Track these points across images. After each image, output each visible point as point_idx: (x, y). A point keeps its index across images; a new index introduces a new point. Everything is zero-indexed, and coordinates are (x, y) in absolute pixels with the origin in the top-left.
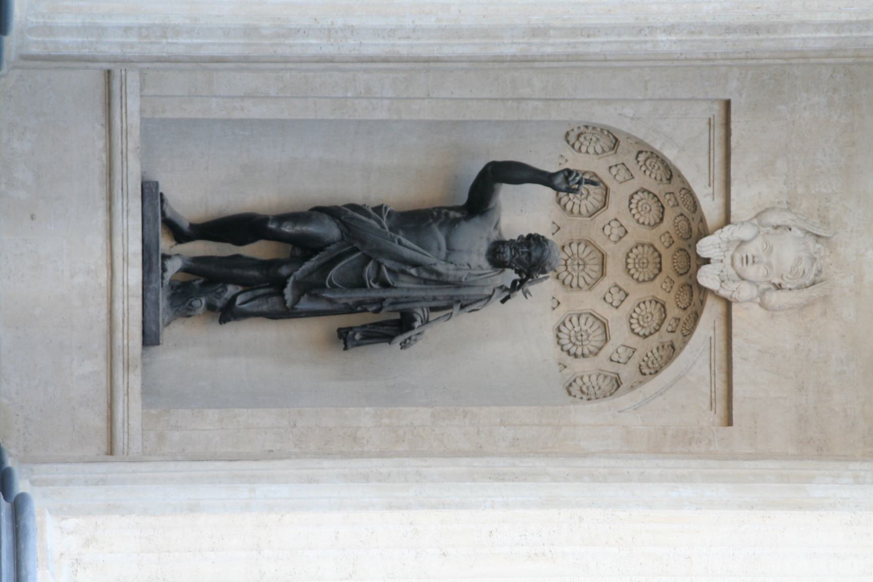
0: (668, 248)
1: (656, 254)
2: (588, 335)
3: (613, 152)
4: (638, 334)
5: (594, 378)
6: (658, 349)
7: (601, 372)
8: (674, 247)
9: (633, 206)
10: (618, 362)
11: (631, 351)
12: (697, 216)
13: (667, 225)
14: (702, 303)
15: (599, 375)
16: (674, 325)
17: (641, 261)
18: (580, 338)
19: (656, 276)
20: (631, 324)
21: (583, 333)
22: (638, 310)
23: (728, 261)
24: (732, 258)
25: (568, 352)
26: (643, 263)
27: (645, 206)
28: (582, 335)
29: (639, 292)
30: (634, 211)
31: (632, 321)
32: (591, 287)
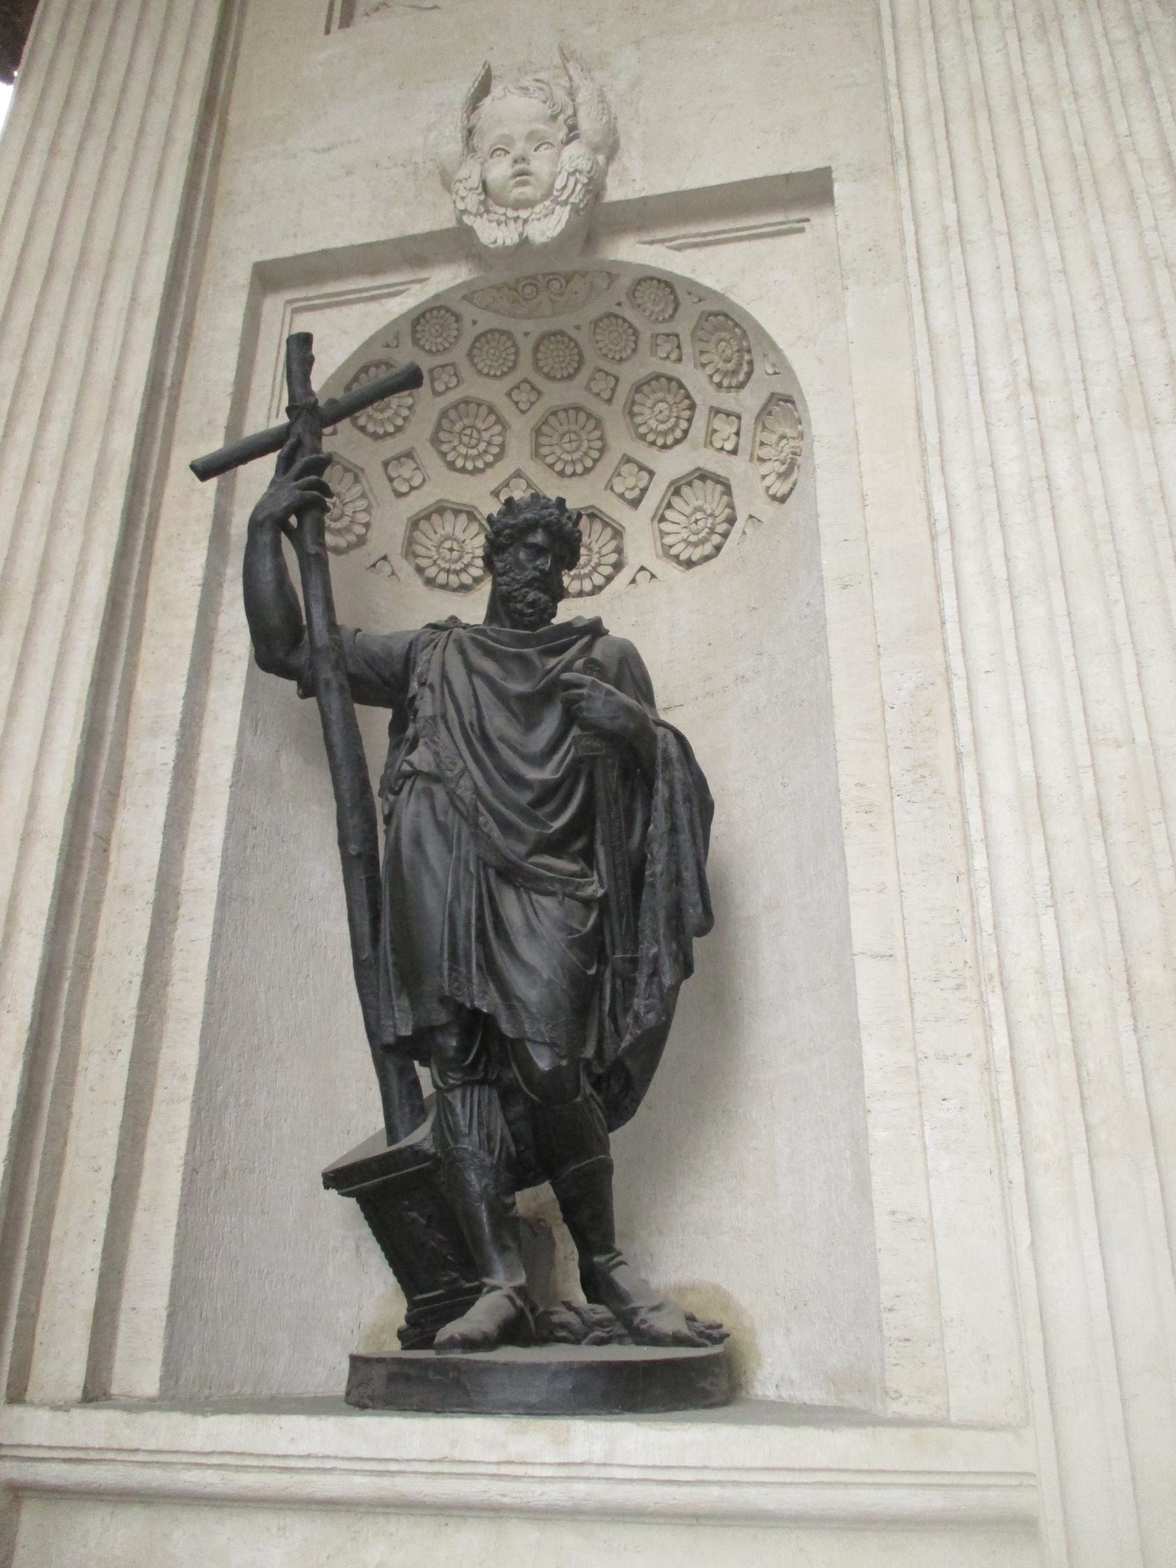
0: (540, 393)
1: (552, 420)
2: (698, 509)
3: (361, 475)
4: (690, 420)
5: (765, 468)
6: (704, 365)
7: (756, 457)
8: (538, 381)
9: (469, 466)
10: (737, 434)
11: (718, 423)
12: (468, 311)
13: (493, 391)
14: (611, 274)
15: (762, 460)
16: (668, 347)
17: (567, 446)
18: (701, 523)
19: (590, 416)
20: (677, 442)
21: (693, 519)
22: (650, 438)
23: (524, 214)
24: (519, 205)
25: (725, 535)
26: (570, 441)
27: (466, 439)
28: (696, 521)
29: (621, 443)
30: (480, 464)
31: (670, 440)
32: (618, 534)
